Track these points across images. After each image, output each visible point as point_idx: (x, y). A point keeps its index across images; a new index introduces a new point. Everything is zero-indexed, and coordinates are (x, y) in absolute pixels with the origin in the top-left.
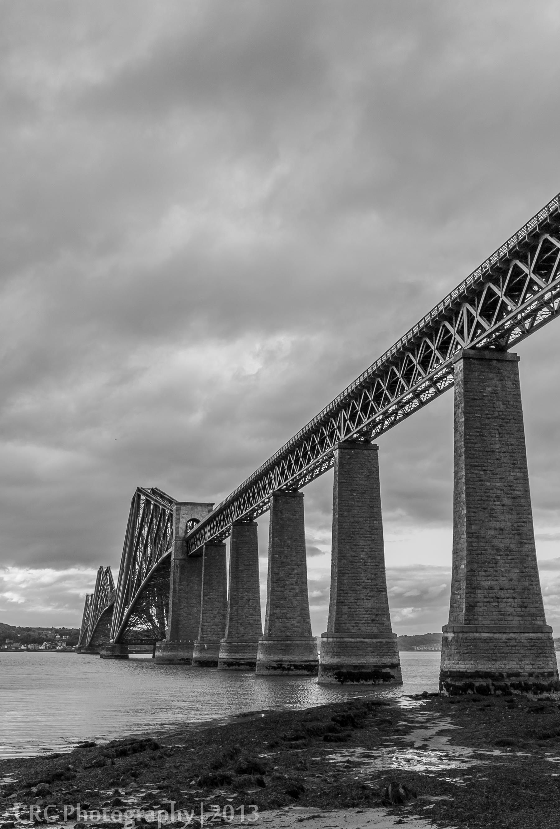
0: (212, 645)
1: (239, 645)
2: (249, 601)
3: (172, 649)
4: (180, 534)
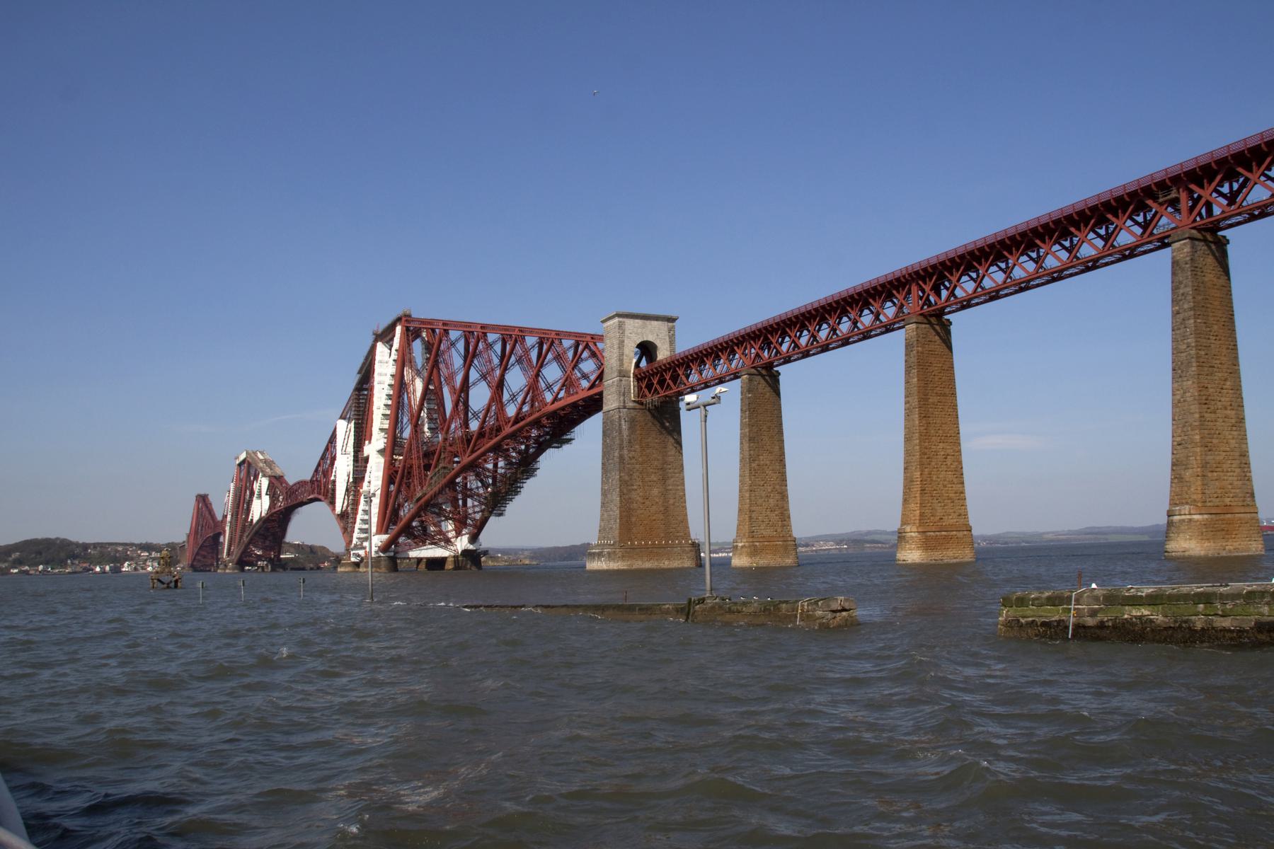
0: (766, 543)
1: (937, 536)
2: (946, 458)
3: (623, 556)
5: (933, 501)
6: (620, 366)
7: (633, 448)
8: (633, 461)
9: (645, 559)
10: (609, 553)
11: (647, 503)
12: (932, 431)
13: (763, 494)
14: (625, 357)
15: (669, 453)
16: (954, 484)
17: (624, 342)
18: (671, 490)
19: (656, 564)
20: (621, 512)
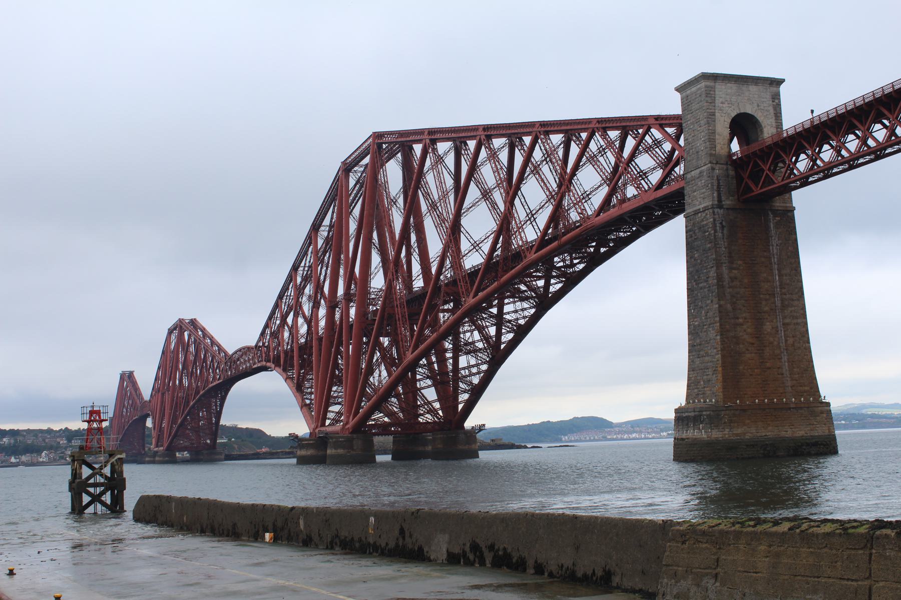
3: (731, 421)
4: (718, 147)
6: (711, 148)
10: (709, 416)
14: (717, 137)
17: (714, 115)
20: (723, 356)
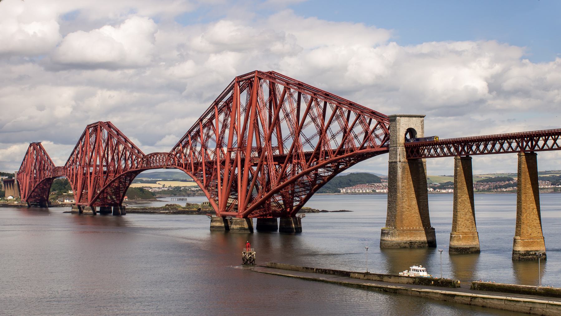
0: (465, 235)
1: (529, 241)
5: (527, 227)
7: (403, 182)
8: (404, 188)
9: (409, 236)
11: (410, 208)
12: (528, 199)
13: (464, 213)
14: (400, 137)
15: (421, 184)
16: (536, 220)
18: (421, 202)
19: (414, 238)
